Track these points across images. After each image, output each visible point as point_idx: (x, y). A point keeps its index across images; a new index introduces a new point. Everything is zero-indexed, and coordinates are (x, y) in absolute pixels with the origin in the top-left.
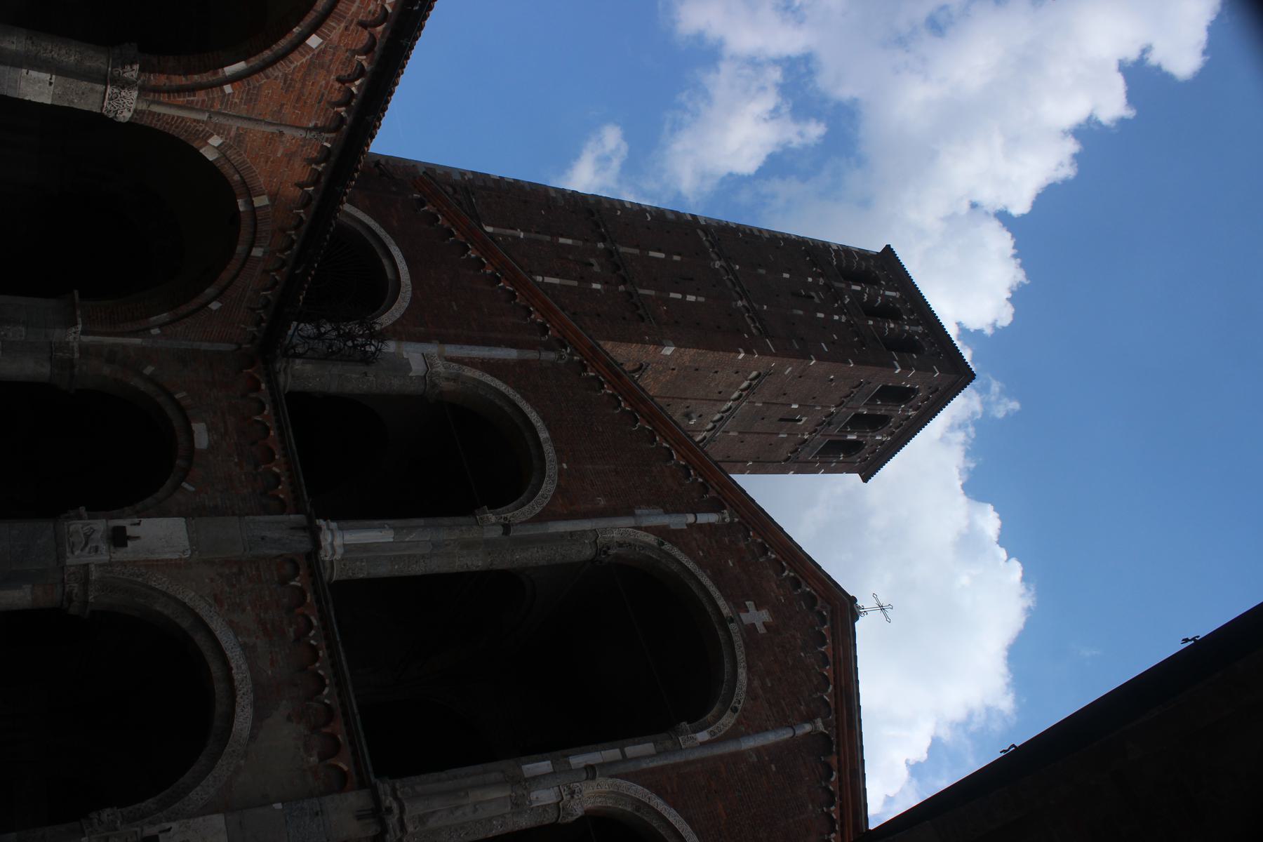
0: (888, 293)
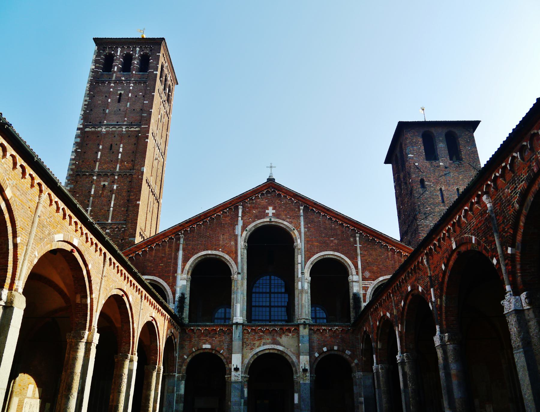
0: (119, 54)
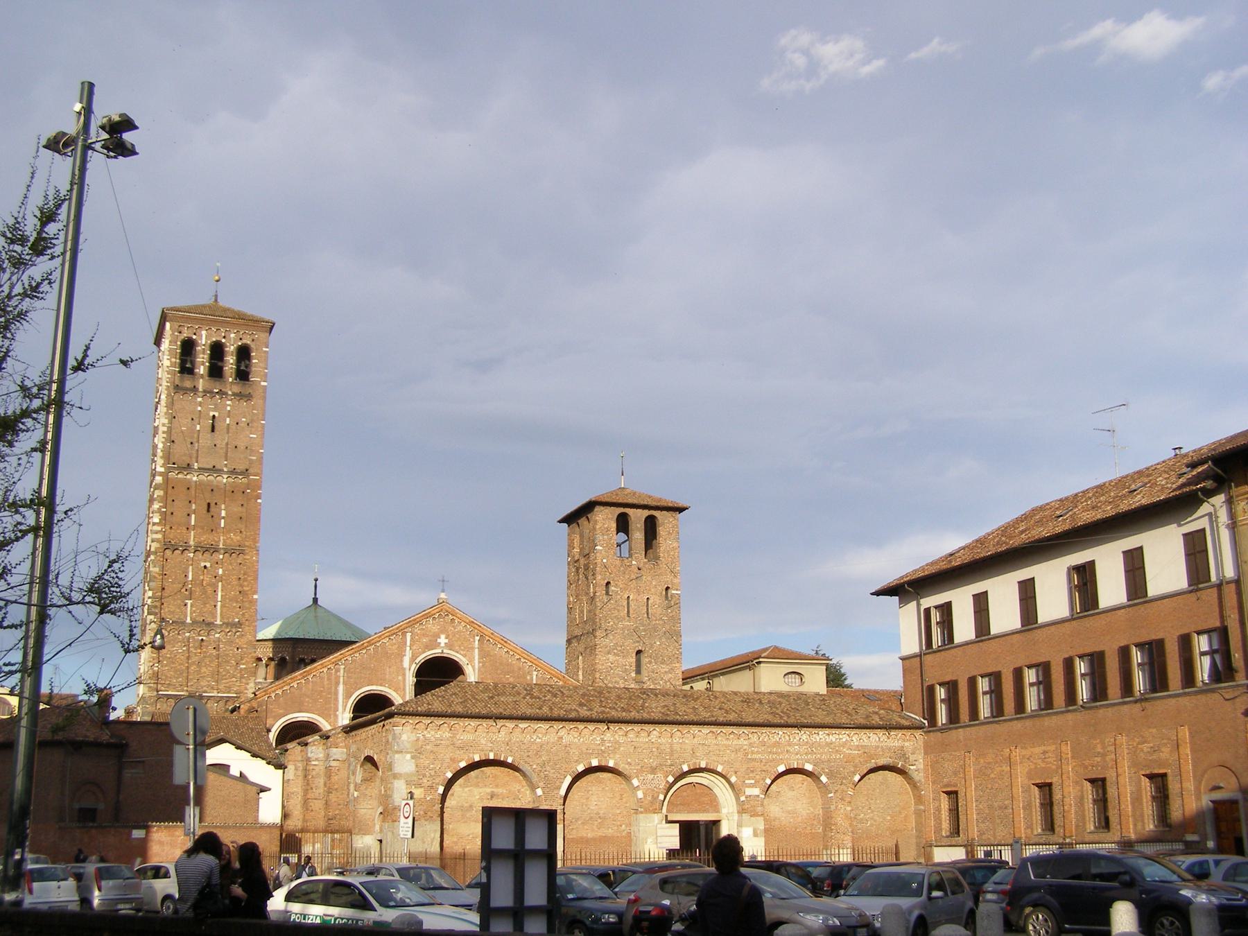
0: (204, 343)
